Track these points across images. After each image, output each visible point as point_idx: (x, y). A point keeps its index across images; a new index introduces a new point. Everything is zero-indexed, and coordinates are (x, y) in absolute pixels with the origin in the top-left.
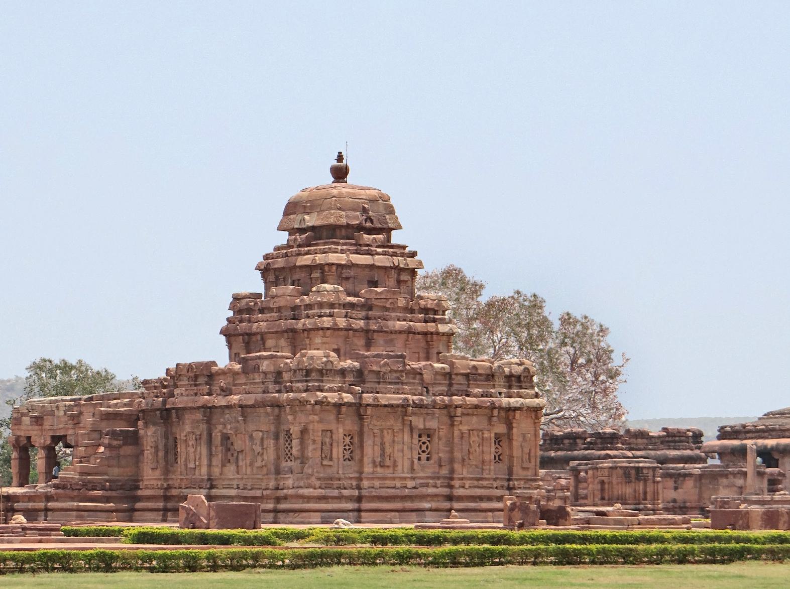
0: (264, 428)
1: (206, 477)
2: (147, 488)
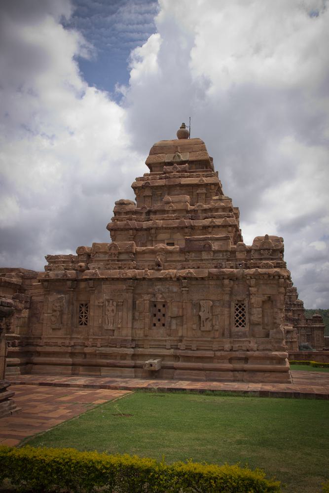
0: (213, 297)
1: (130, 338)
2: (47, 344)
